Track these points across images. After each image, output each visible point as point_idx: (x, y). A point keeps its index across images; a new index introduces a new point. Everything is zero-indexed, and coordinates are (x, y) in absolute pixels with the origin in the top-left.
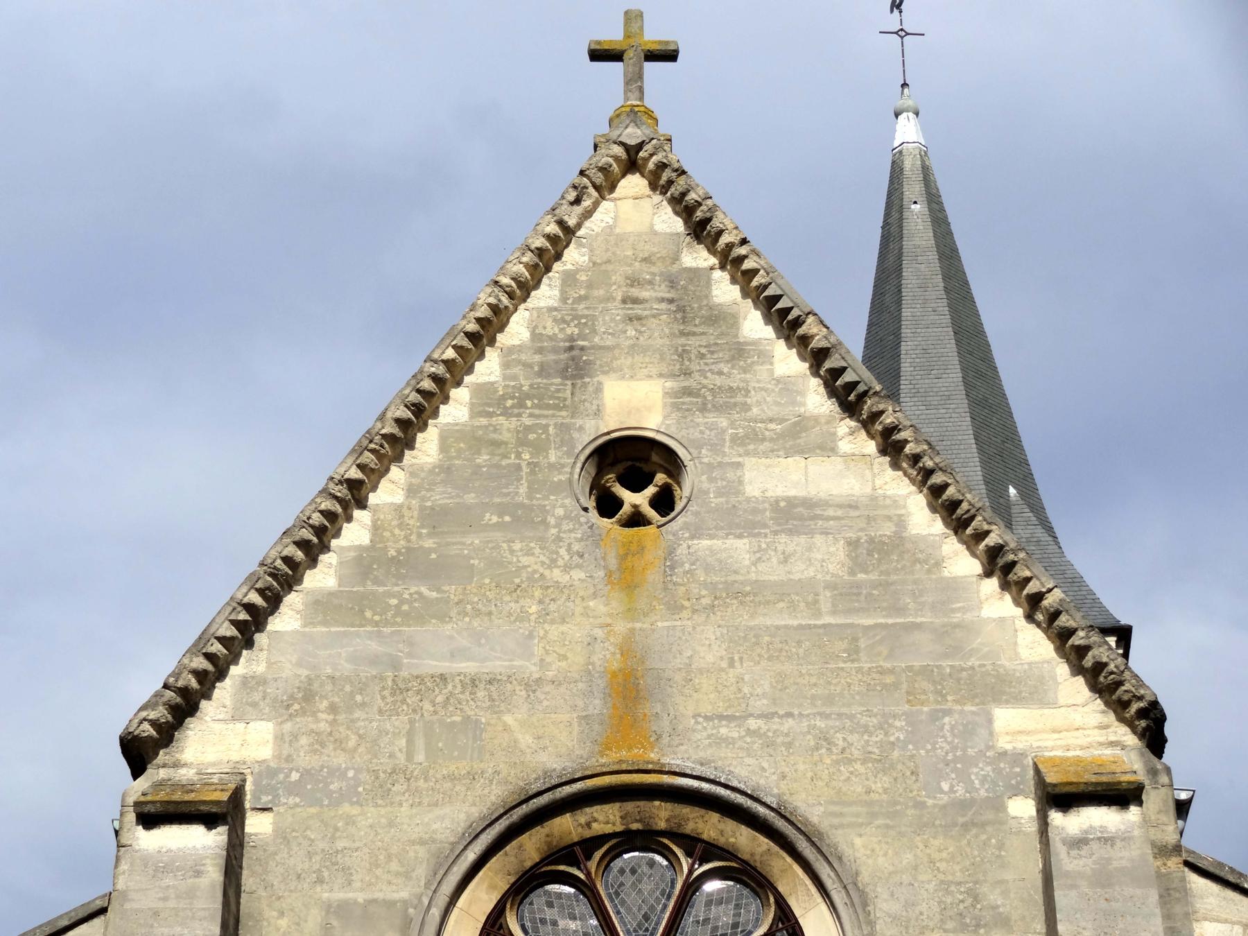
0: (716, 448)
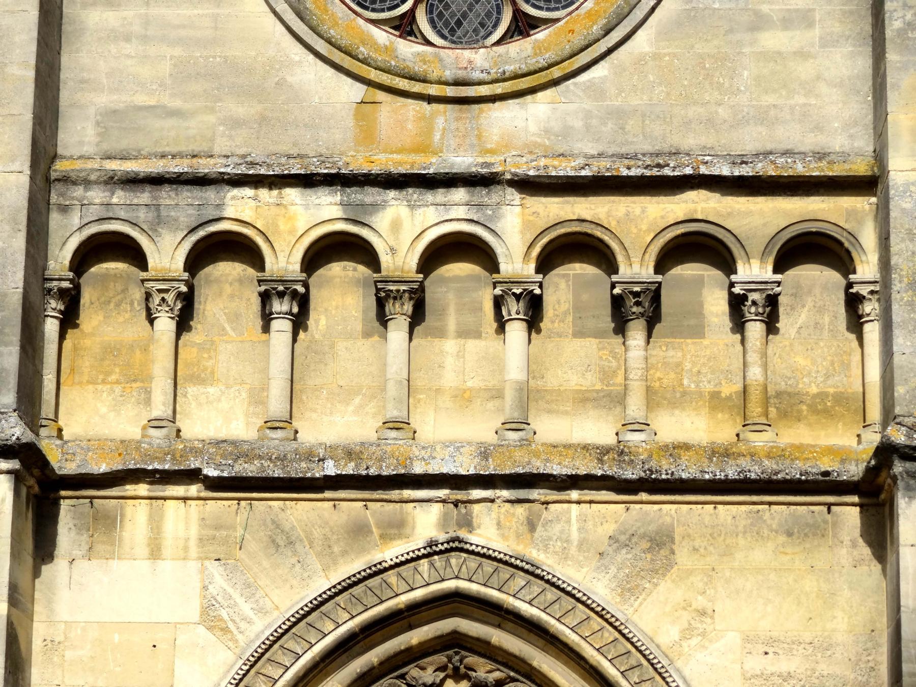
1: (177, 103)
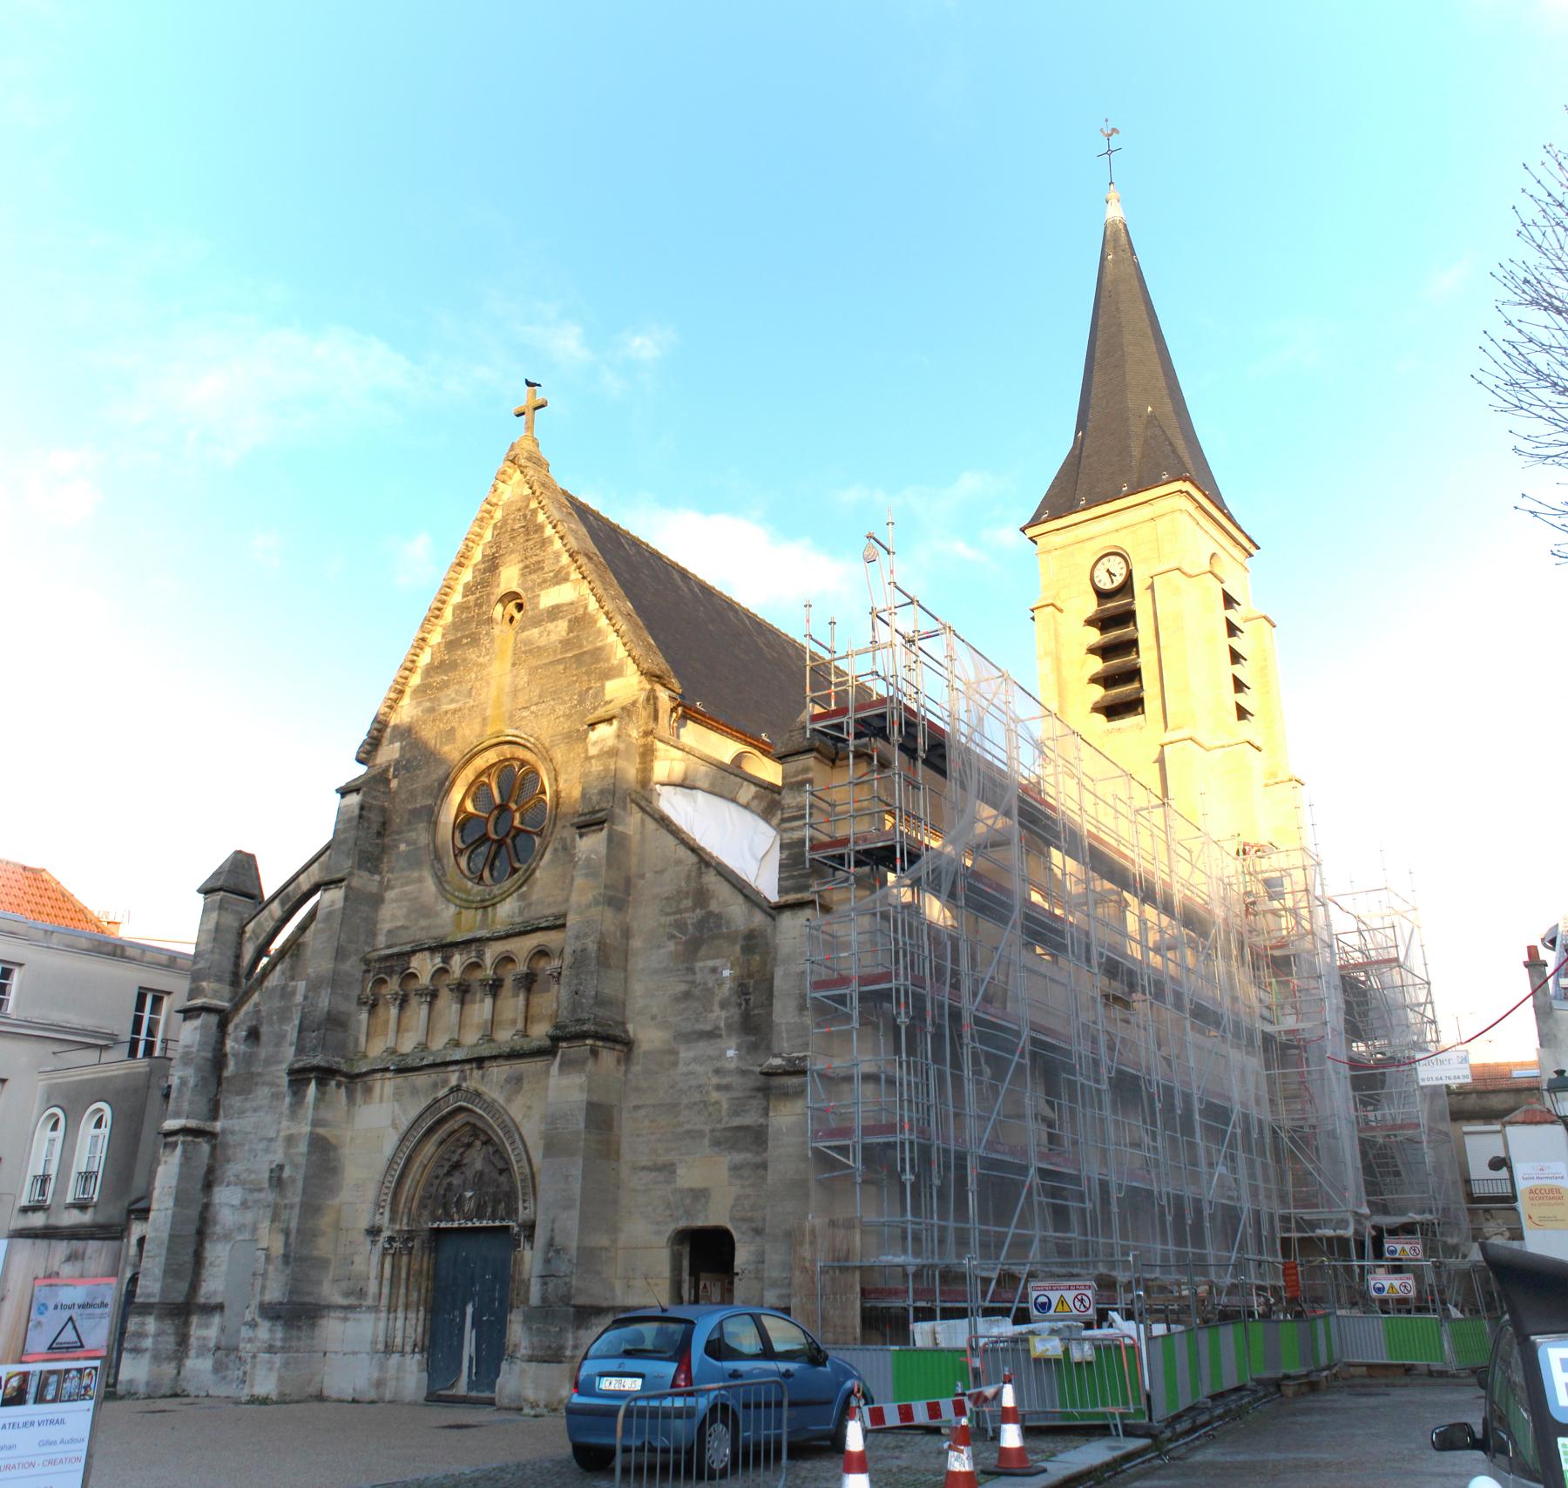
0: (532, 589)
1: (407, 924)
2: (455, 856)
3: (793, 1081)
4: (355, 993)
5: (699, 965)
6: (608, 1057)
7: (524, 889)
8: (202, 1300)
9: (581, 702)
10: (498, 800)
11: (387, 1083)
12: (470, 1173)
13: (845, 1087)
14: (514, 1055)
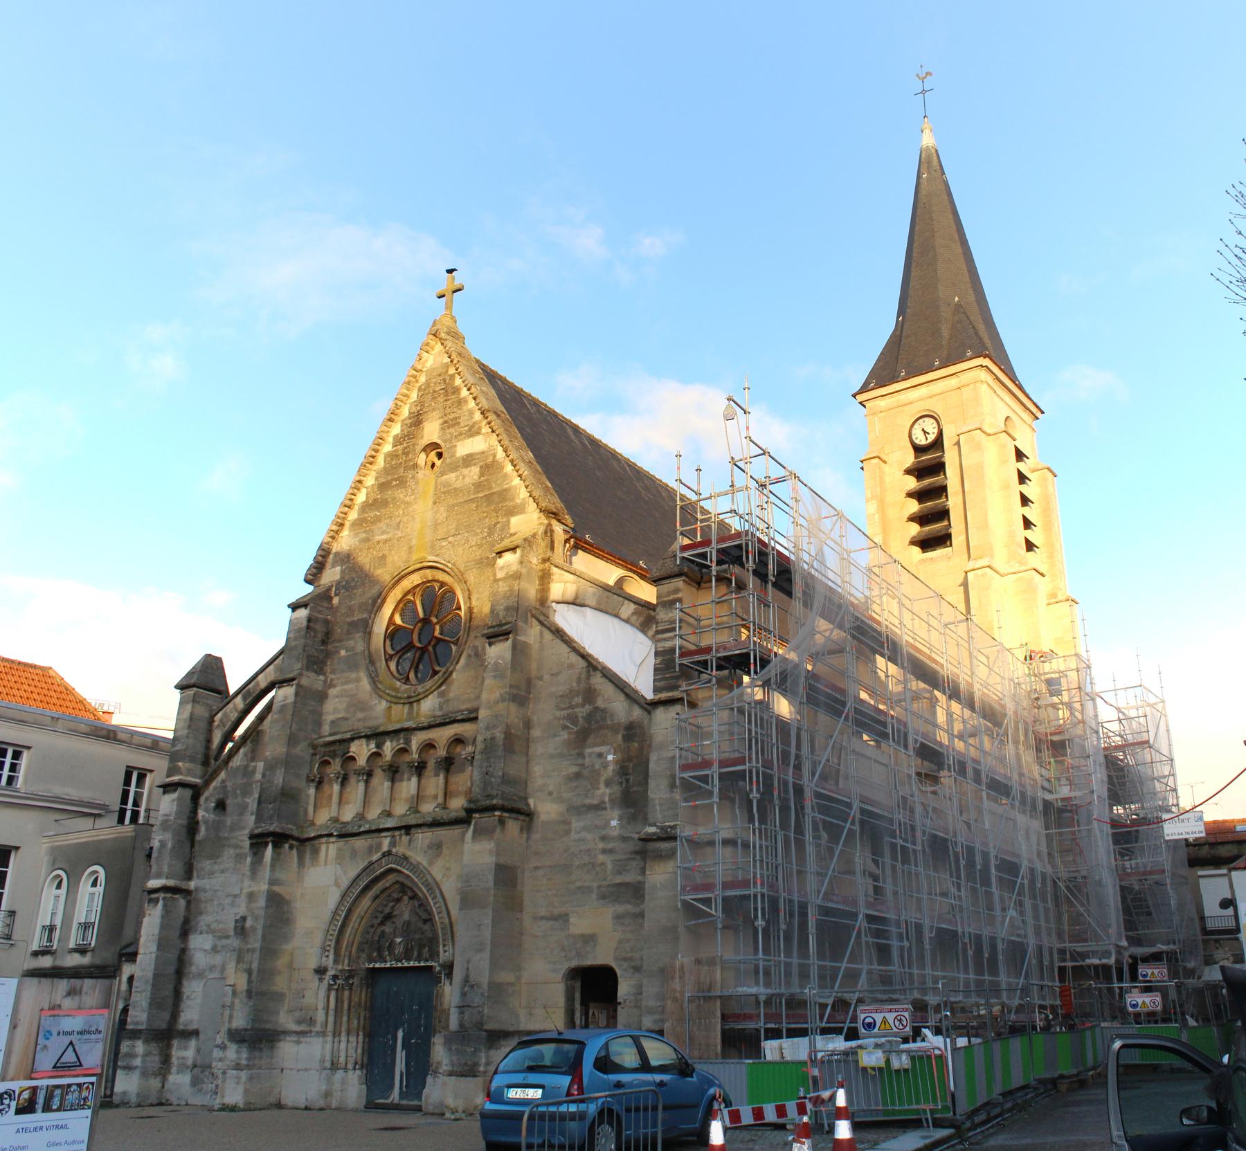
0: (450, 440)
1: (347, 716)
2: (386, 660)
3: (665, 846)
4: (305, 771)
5: (588, 751)
6: (513, 826)
7: (443, 688)
8: (181, 1027)
9: (490, 534)
10: (421, 615)
11: (331, 846)
12: (399, 923)
13: (708, 850)
14: (436, 824)
